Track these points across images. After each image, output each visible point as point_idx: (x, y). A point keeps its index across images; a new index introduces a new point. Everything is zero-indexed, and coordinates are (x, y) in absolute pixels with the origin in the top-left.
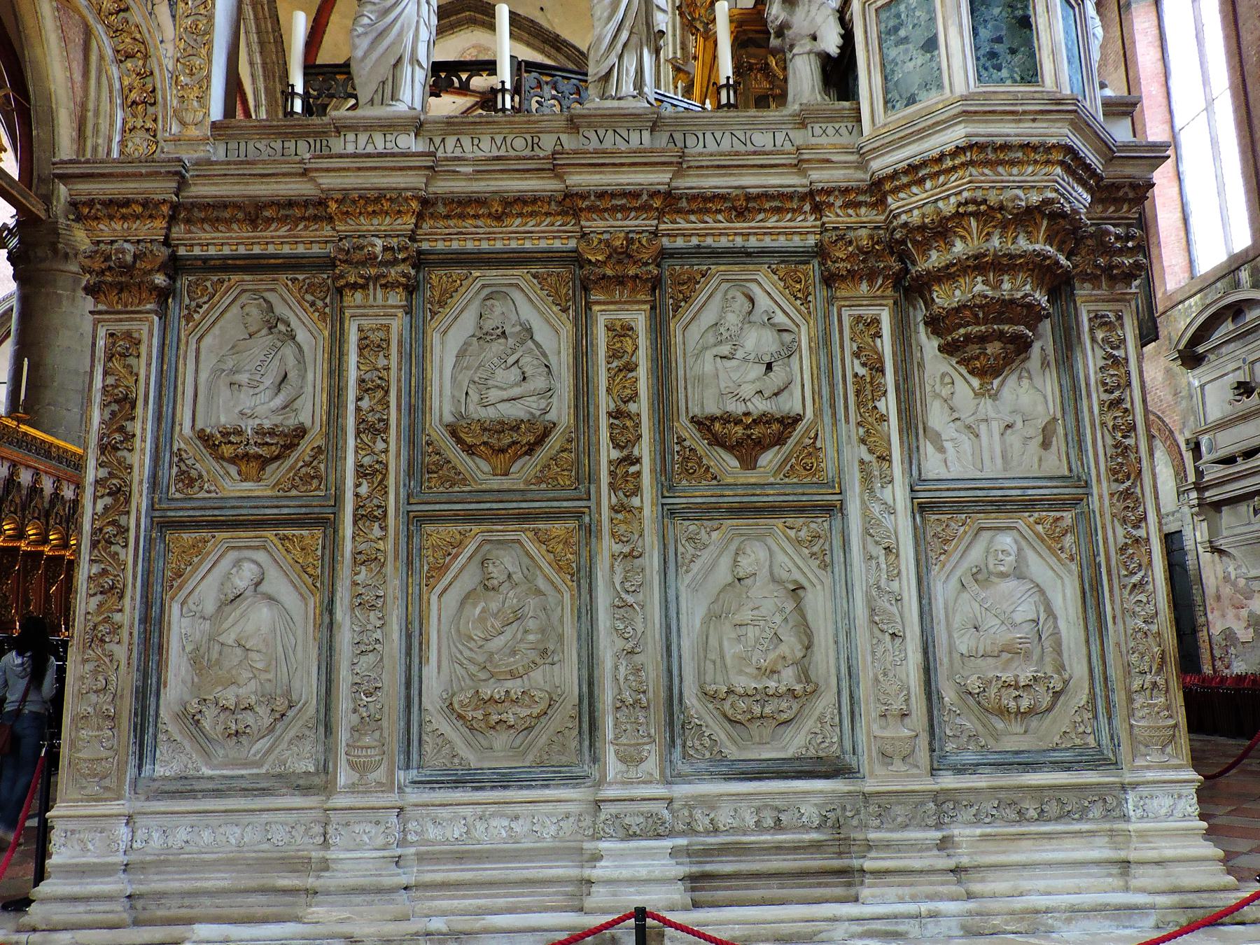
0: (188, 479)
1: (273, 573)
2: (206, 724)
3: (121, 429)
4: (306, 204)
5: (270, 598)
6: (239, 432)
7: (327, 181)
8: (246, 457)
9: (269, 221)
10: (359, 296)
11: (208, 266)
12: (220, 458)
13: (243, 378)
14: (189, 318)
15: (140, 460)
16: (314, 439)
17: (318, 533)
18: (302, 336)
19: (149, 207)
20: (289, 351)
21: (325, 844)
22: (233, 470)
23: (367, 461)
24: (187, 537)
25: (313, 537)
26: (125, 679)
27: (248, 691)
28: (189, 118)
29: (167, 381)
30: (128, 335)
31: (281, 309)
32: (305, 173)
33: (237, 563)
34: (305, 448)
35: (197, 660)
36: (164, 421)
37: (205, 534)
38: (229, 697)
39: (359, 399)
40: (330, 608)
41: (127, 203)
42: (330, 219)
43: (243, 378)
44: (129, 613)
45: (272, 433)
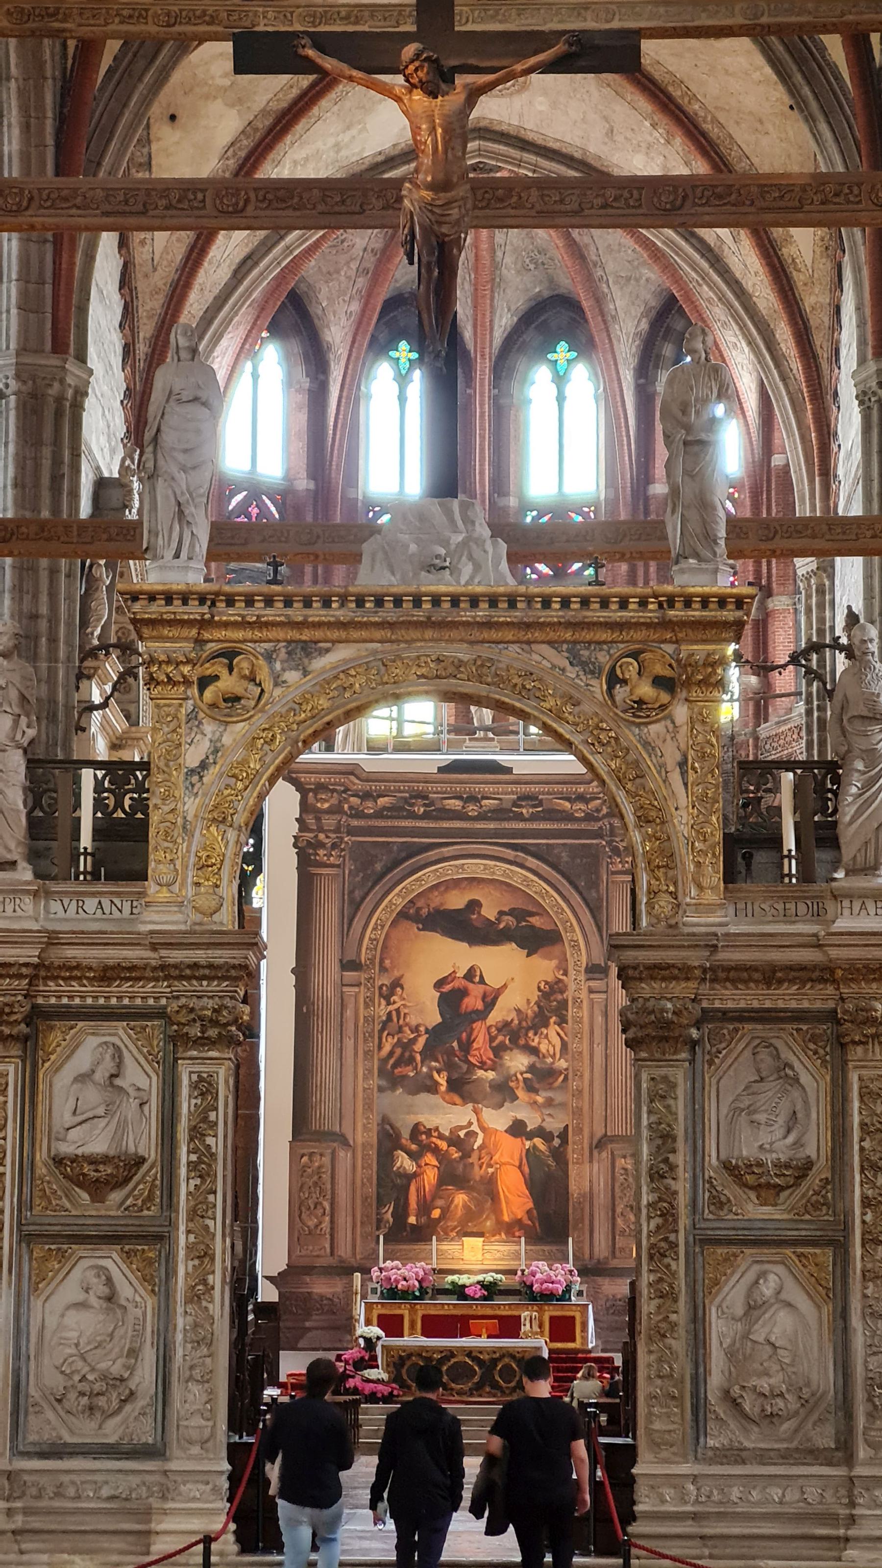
0: (718, 1203)
1: (790, 1282)
2: (747, 1407)
3: (666, 1161)
4: (814, 968)
5: (789, 1305)
6: (760, 1164)
7: (834, 953)
8: (768, 1186)
9: (780, 982)
10: (860, 1049)
11: (725, 1016)
12: (745, 1185)
13: (761, 1117)
14: (711, 1063)
15: (682, 1186)
16: (821, 1171)
17: (829, 1252)
18: (805, 1079)
19: (684, 972)
20: (796, 1094)
21: (852, 1504)
22: (753, 1195)
23: (870, 1193)
24: (721, 1251)
25: (827, 1256)
26: (683, 1366)
27: (776, 1380)
28: (705, 883)
29: (697, 1116)
30: (665, 1079)
31: (787, 1055)
32: (819, 946)
33: (763, 1274)
34: (814, 1180)
35: (731, 1354)
36: (697, 1152)
37: (734, 1249)
38: (764, 1385)
39: (862, 1140)
40: (844, 1314)
41: (669, 967)
42: (834, 981)
43: (761, 1117)
44: (681, 1315)
45: (787, 1166)
